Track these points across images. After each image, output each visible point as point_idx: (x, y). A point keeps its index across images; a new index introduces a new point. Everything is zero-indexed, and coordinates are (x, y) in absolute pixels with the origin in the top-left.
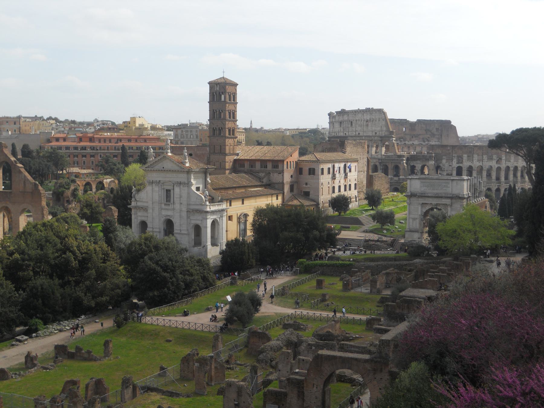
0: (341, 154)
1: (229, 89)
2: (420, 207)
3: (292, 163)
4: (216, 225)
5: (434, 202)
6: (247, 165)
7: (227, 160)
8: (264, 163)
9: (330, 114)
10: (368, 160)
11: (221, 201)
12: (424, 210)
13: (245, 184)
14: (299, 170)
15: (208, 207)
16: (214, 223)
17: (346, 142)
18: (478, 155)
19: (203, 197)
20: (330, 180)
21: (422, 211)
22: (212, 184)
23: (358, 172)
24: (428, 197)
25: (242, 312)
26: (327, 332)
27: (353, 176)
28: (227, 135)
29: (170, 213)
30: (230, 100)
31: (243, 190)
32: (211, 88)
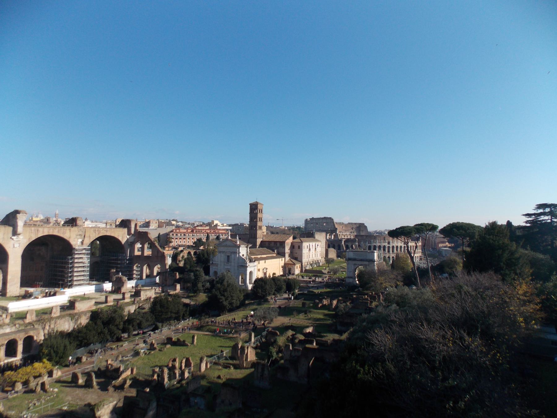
1: (259, 207)
8: (275, 242)
11: (254, 261)
14: (292, 247)
22: (250, 253)
27: (319, 249)
29: (229, 267)
32: (251, 207)
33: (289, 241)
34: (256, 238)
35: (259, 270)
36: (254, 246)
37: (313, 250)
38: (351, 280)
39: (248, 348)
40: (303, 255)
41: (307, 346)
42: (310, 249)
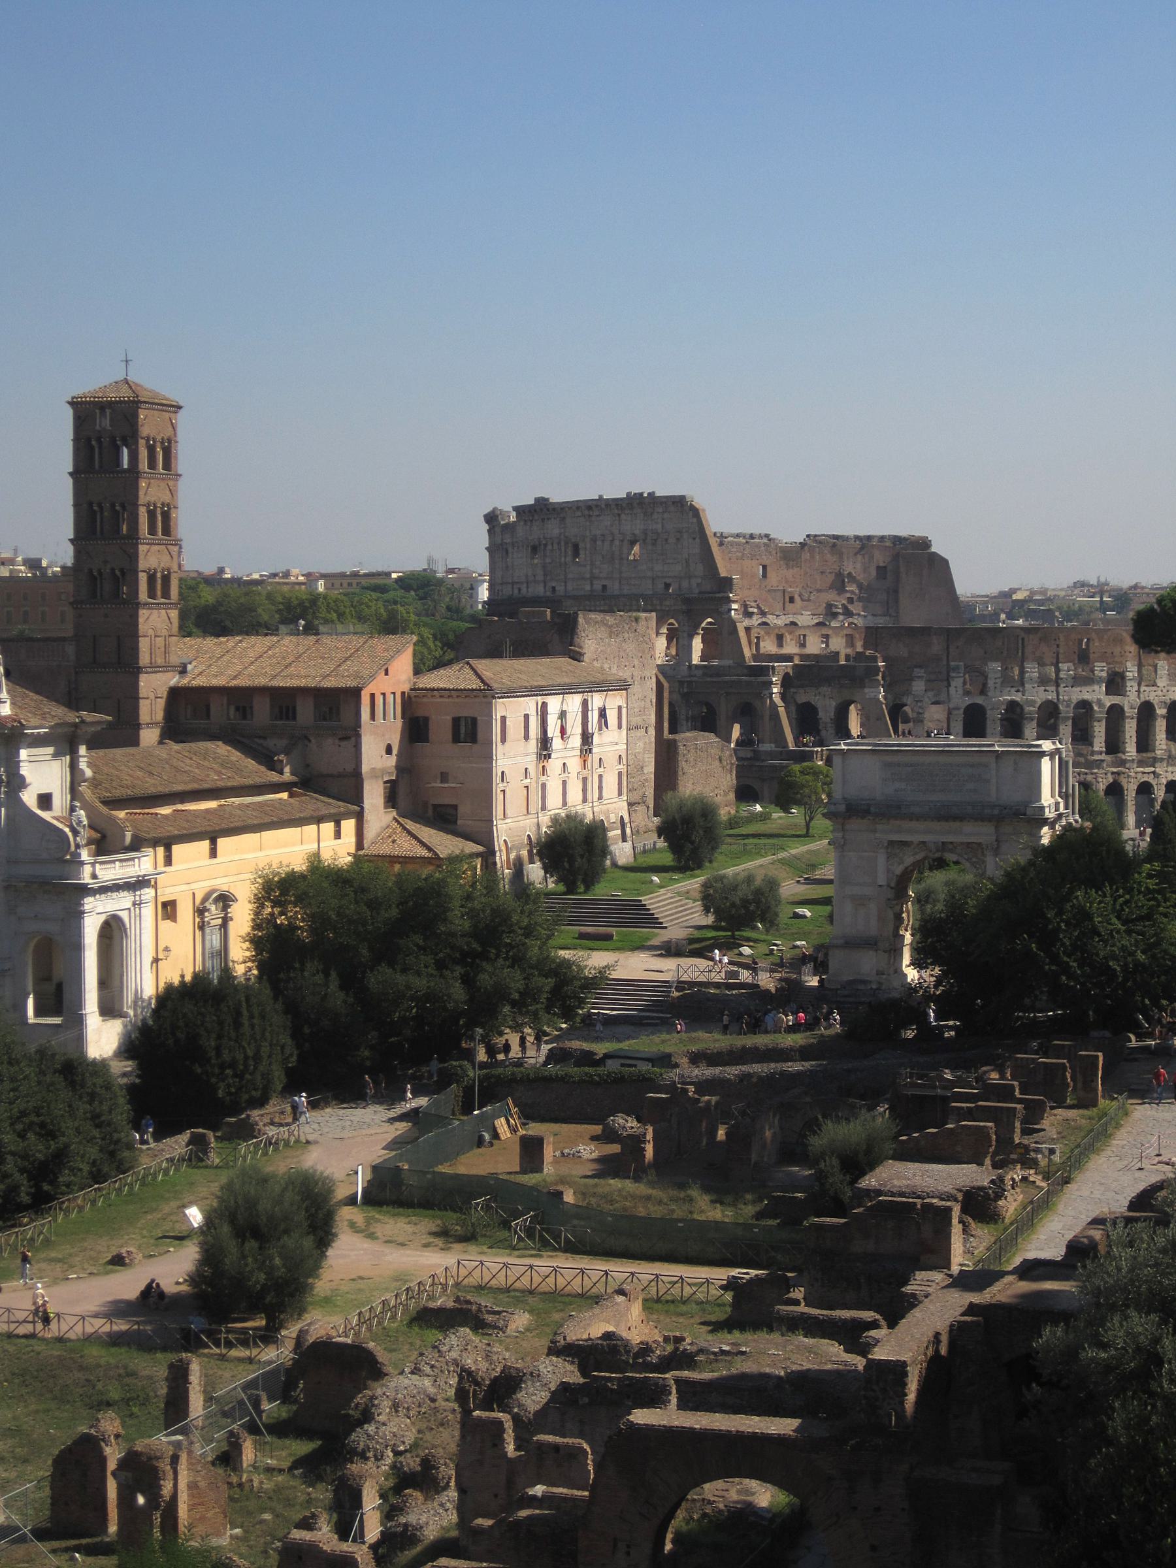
0: (563, 661)
1: (149, 424)
2: (881, 859)
3: (390, 698)
4: (116, 933)
5: (933, 834)
6: (220, 712)
7: (143, 692)
8: (284, 701)
9: (491, 518)
10: (659, 683)
11: (136, 845)
12: (899, 870)
13: (214, 780)
14: (416, 729)
15: (87, 870)
16: (112, 930)
17: (581, 620)
18: (1041, 664)
19: (67, 830)
20: (530, 761)
21: (888, 871)
22: (95, 783)
23: (629, 729)
24: (912, 817)
25: (257, 1265)
26: (608, 1336)
27: (611, 743)
28: (143, 596)
30: (152, 464)
31: (212, 804)
33: (391, 674)
34: (133, 669)
35: (169, 909)
36: (123, 731)
37: (566, 751)
38: (868, 964)
39: (175, 1460)
40: (498, 786)
41: (641, 1416)
42: (545, 743)
